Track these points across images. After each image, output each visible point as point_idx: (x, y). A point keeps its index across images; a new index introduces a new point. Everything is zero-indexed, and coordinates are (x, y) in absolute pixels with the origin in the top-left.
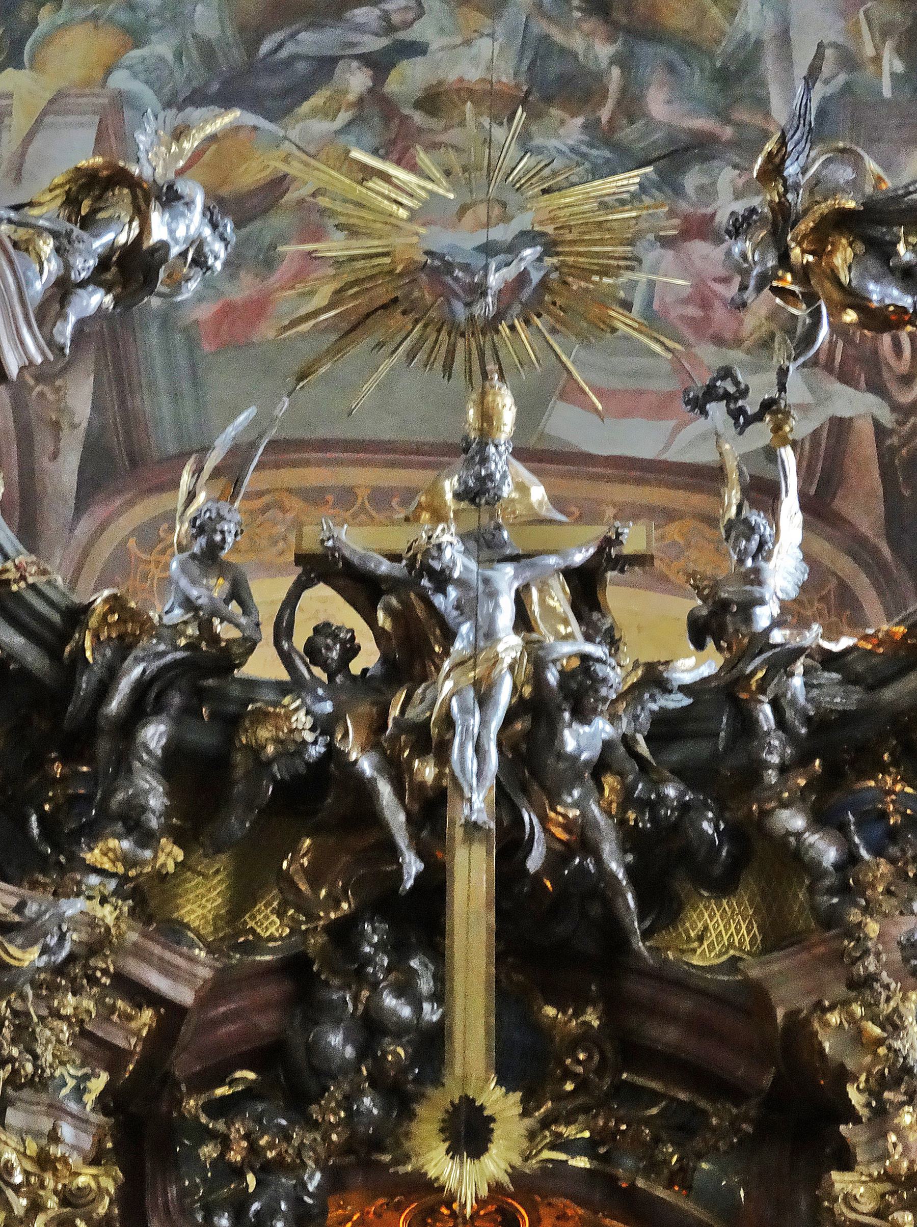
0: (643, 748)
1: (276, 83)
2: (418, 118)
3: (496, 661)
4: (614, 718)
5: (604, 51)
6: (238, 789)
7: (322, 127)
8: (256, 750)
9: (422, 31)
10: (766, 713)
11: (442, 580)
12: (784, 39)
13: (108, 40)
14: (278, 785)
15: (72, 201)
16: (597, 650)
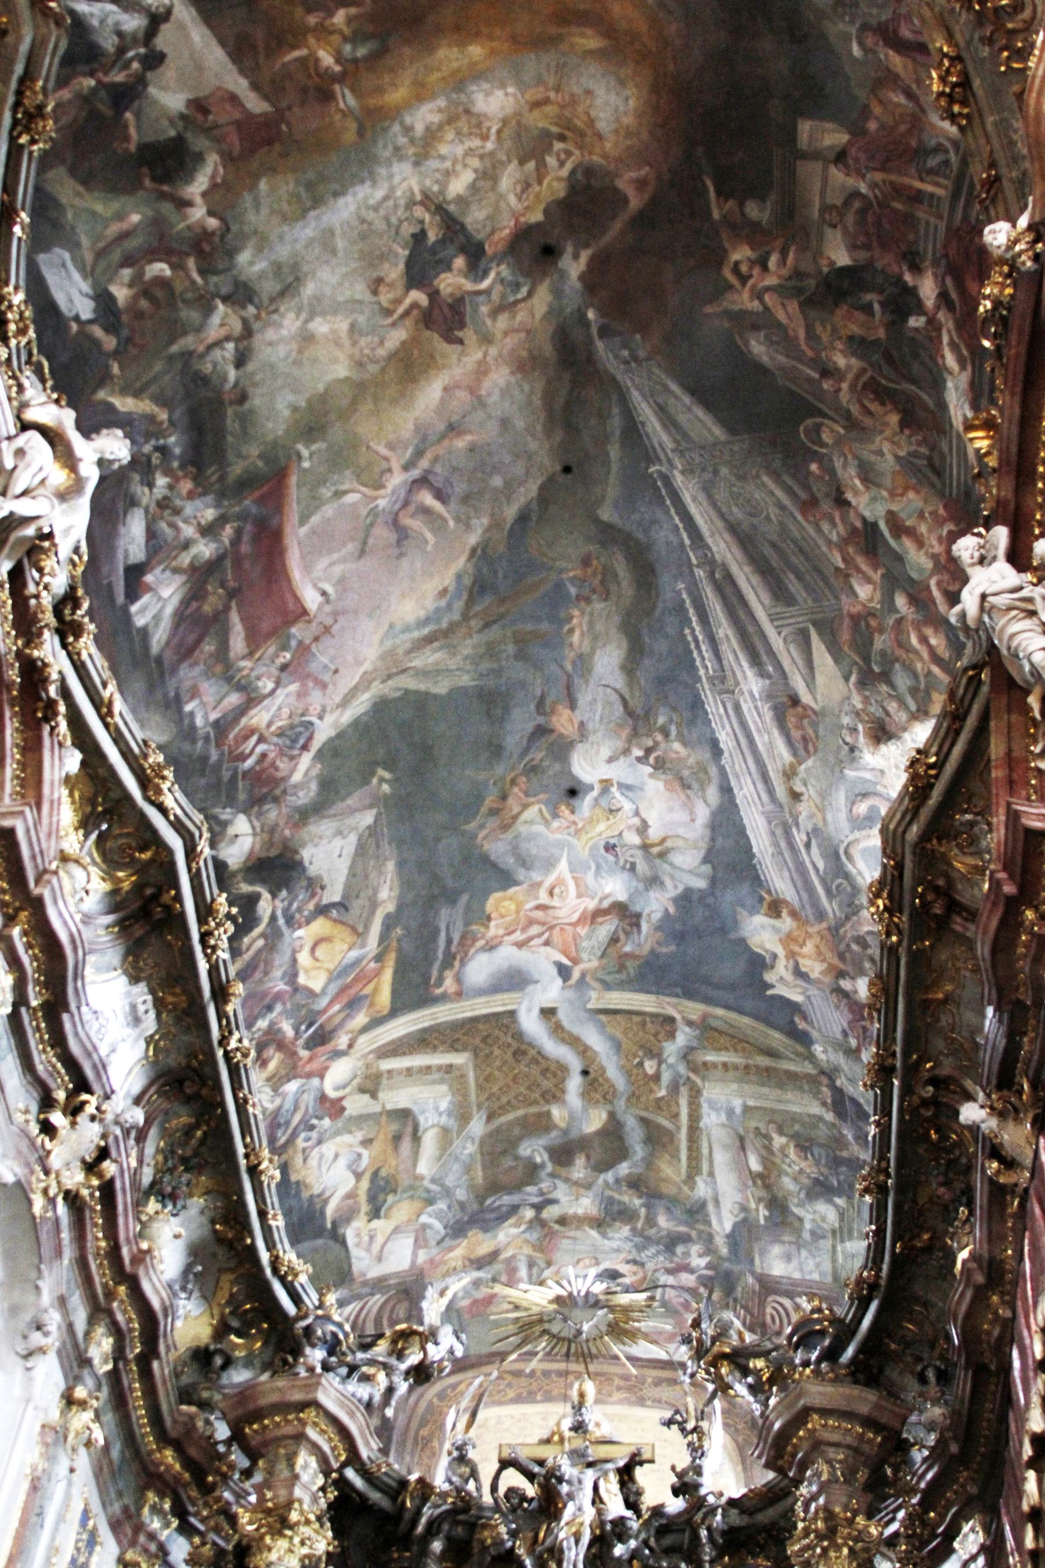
0: (652, 1542)
1: (493, 1216)
2: (557, 1227)
3: (582, 1524)
4: (636, 1537)
5: (637, 1202)
6: (475, 1559)
7: (514, 1231)
8: (482, 1542)
9: (558, 1194)
10: (704, 1533)
11: (560, 1480)
12: (717, 1202)
13: (418, 1204)
14: (493, 1558)
15: (394, 1342)
16: (629, 1514)
